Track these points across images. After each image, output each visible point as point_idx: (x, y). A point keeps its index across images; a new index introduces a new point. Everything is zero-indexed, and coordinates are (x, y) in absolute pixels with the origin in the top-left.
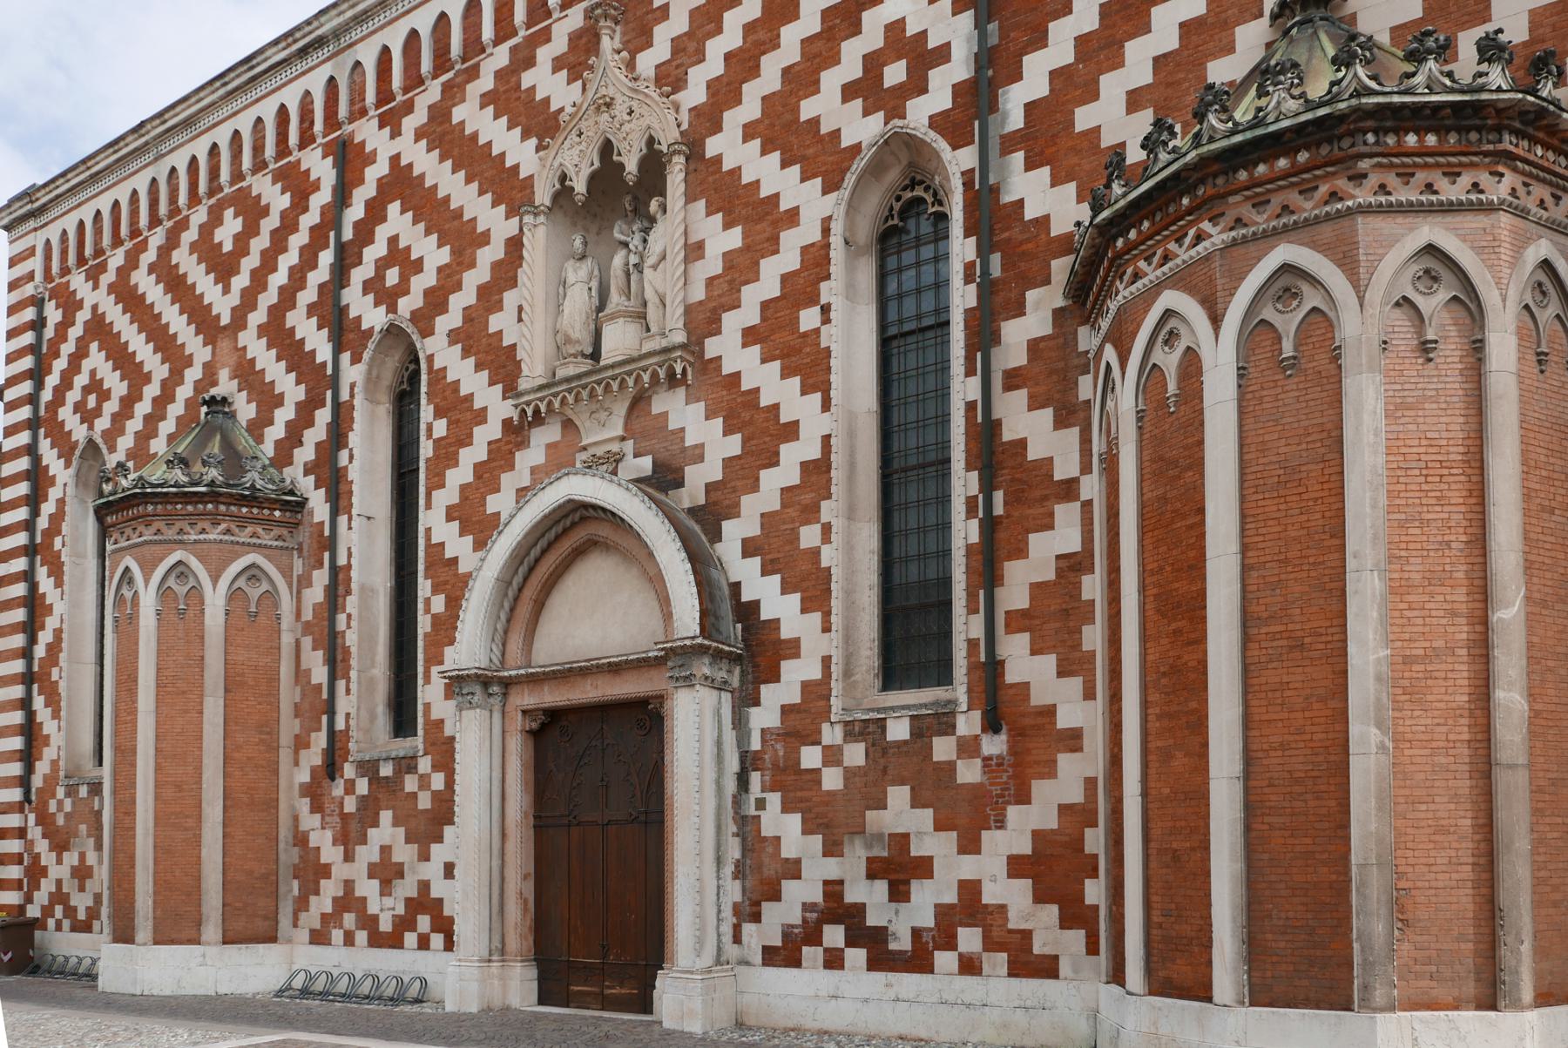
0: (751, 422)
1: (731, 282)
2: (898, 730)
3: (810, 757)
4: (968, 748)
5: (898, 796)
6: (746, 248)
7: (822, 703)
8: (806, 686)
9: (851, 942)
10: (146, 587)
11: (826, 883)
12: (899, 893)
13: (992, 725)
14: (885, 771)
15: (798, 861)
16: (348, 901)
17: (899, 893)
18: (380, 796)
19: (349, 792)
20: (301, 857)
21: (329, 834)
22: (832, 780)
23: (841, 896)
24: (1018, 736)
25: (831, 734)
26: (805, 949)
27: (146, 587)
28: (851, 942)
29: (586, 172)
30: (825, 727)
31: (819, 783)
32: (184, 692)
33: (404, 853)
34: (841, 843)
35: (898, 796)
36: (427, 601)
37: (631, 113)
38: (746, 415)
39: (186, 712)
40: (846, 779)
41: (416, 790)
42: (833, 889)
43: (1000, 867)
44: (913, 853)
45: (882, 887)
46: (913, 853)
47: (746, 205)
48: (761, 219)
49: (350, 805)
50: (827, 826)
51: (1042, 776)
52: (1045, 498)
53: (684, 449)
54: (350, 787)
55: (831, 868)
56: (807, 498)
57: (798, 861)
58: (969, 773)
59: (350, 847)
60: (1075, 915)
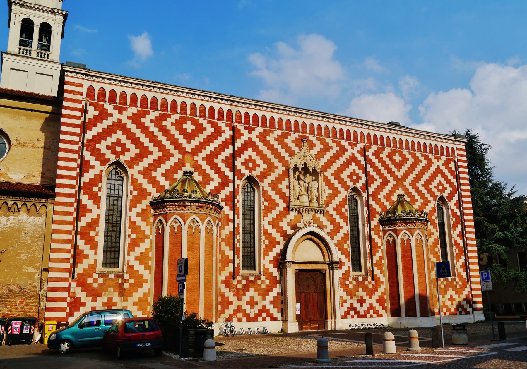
0: (335, 224)
1: (330, 199)
2: (360, 279)
3: (347, 283)
4: (370, 283)
5: (361, 289)
6: (333, 194)
7: (349, 274)
8: (346, 271)
9: (355, 313)
10: (203, 226)
11: (351, 304)
12: (362, 305)
13: (373, 279)
14: (359, 286)
15: (346, 300)
16: (239, 310)
17: (362, 305)
18: (250, 285)
19: (239, 282)
20: (222, 299)
21: (232, 294)
22: (351, 287)
23: (353, 306)
24: (376, 282)
25: (350, 279)
26: (348, 315)
27: (203, 226)
28: (355, 313)
29: (301, 167)
30: (349, 278)
31: (349, 287)
32: (209, 255)
33: (257, 298)
34: (353, 297)
35: (361, 289)
36: (264, 241)
37: (310, 160)
38: (334, 223)
39: (209, 260)
40: (353, 287)
41: (261, 284)
42: (352, 305)
43: (375, 301)
44: (363, 299)
45: (359, 304)
46: (363, 299)
47: (332, 187)
48: (335, 190)
49: (240, 286)
50: (350, 294)
51: (379, 288)
52: (377, 248)
53: (323, 225)
54: (239, 282)
55: (352, 301)
56: (345, 239)
57: (346, 300)
58: (370, 287)
59: (240, 296)
60: (384, 308)
